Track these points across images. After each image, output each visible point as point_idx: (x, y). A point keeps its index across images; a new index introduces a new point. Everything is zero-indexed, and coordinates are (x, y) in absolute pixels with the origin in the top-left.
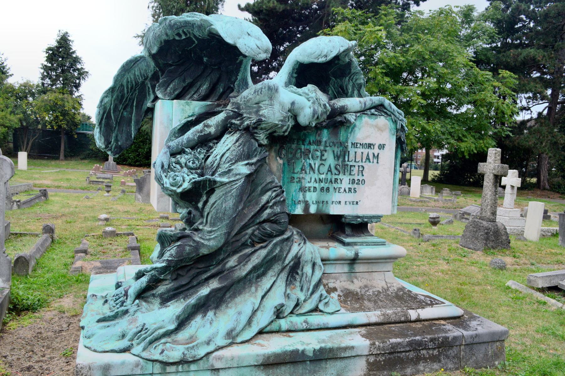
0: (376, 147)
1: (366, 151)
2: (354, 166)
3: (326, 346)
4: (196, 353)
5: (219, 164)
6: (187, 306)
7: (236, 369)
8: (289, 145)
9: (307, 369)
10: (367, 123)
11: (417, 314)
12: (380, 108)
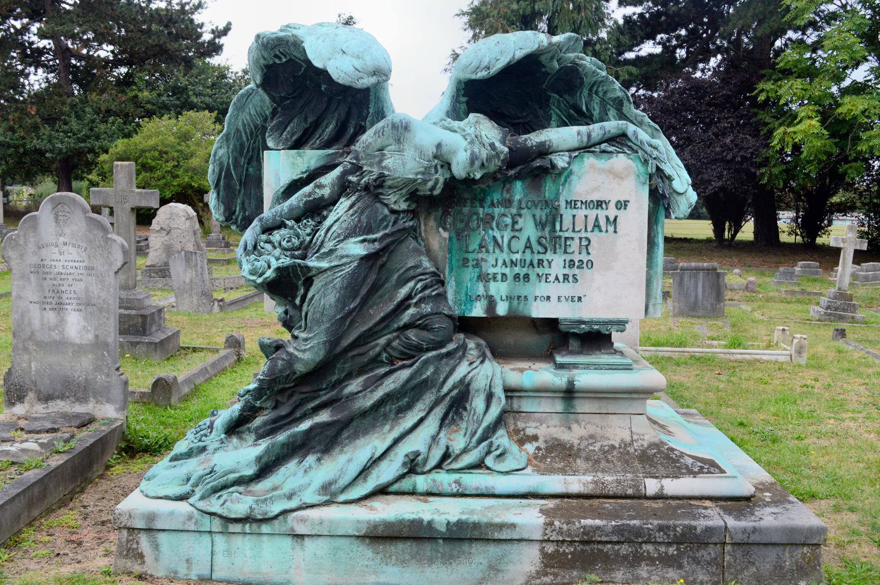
0: (612, 205)
1: (592, 214)
2: (572, 238)
3: (467, 519)
4: (268, 509)
5: (323, 242)
6: (273, 445)
7: (329, 539)
8: (458, 208)
9: (438, 551)
10: (592, 166)
11: (659, 486)
12: (620, 140)
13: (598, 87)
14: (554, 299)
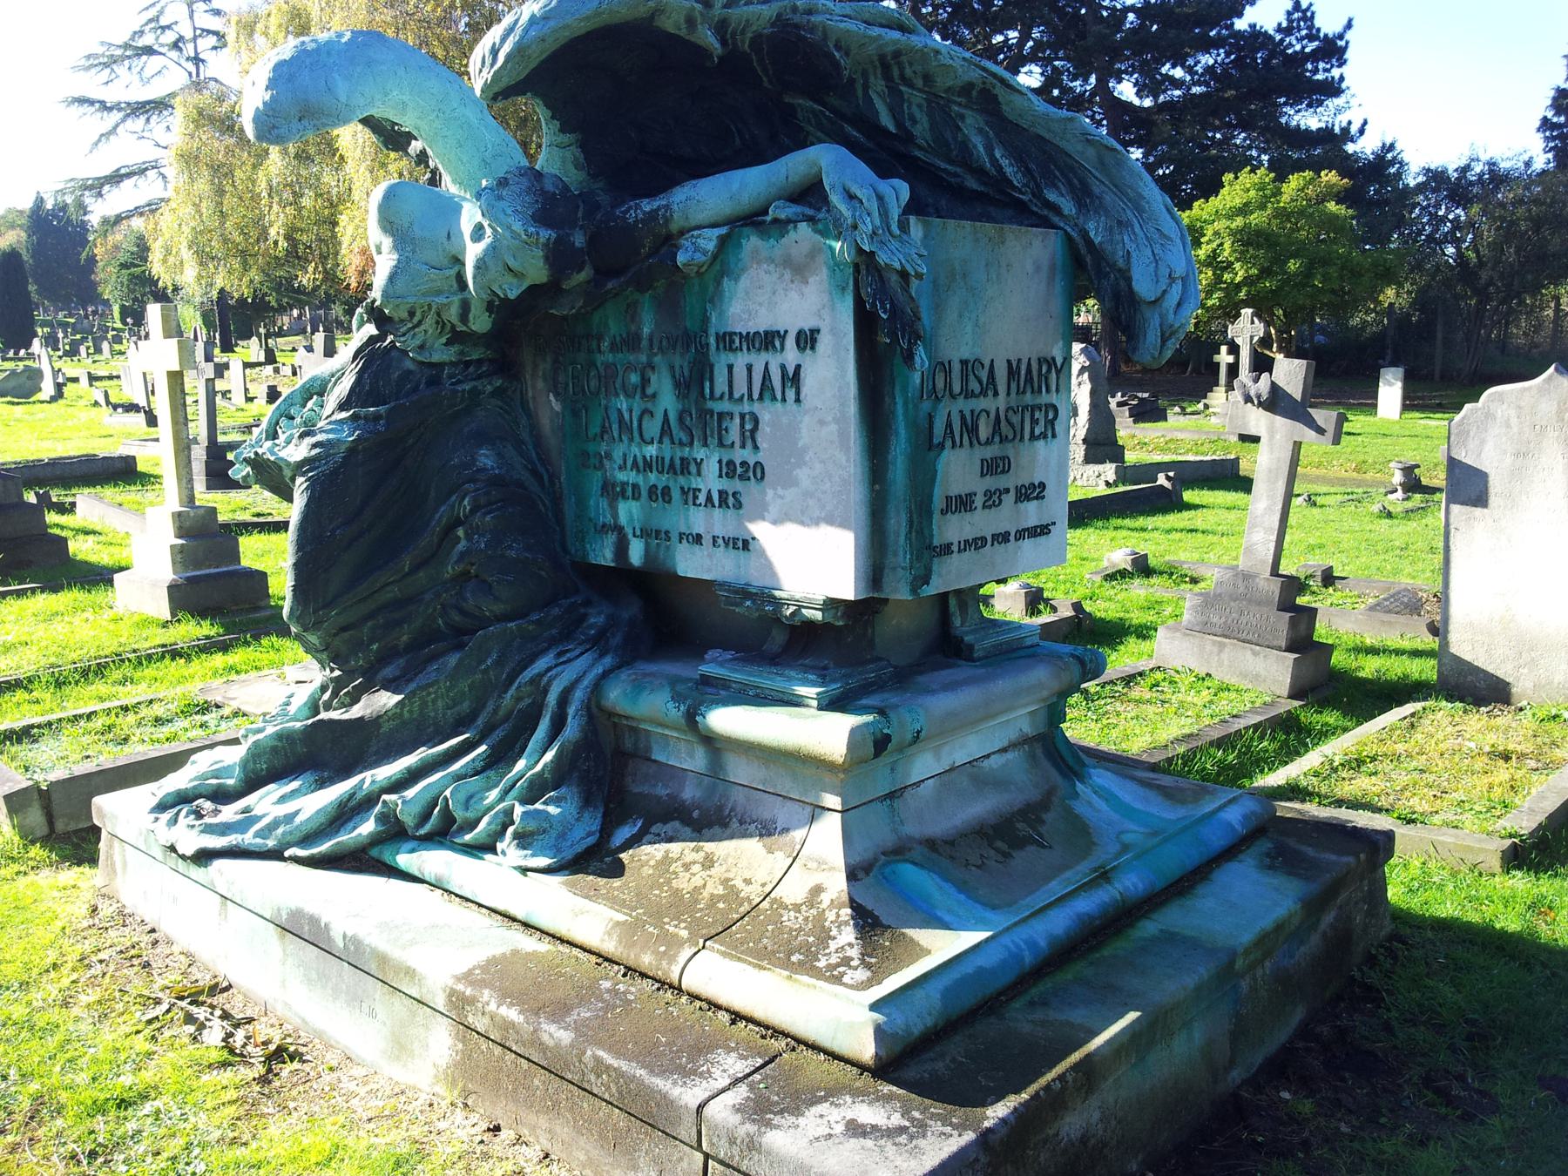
0: (790, 342)
1: (759, 360)
2: (731, 415)
13: (902, 69)
14: (707, 540)
